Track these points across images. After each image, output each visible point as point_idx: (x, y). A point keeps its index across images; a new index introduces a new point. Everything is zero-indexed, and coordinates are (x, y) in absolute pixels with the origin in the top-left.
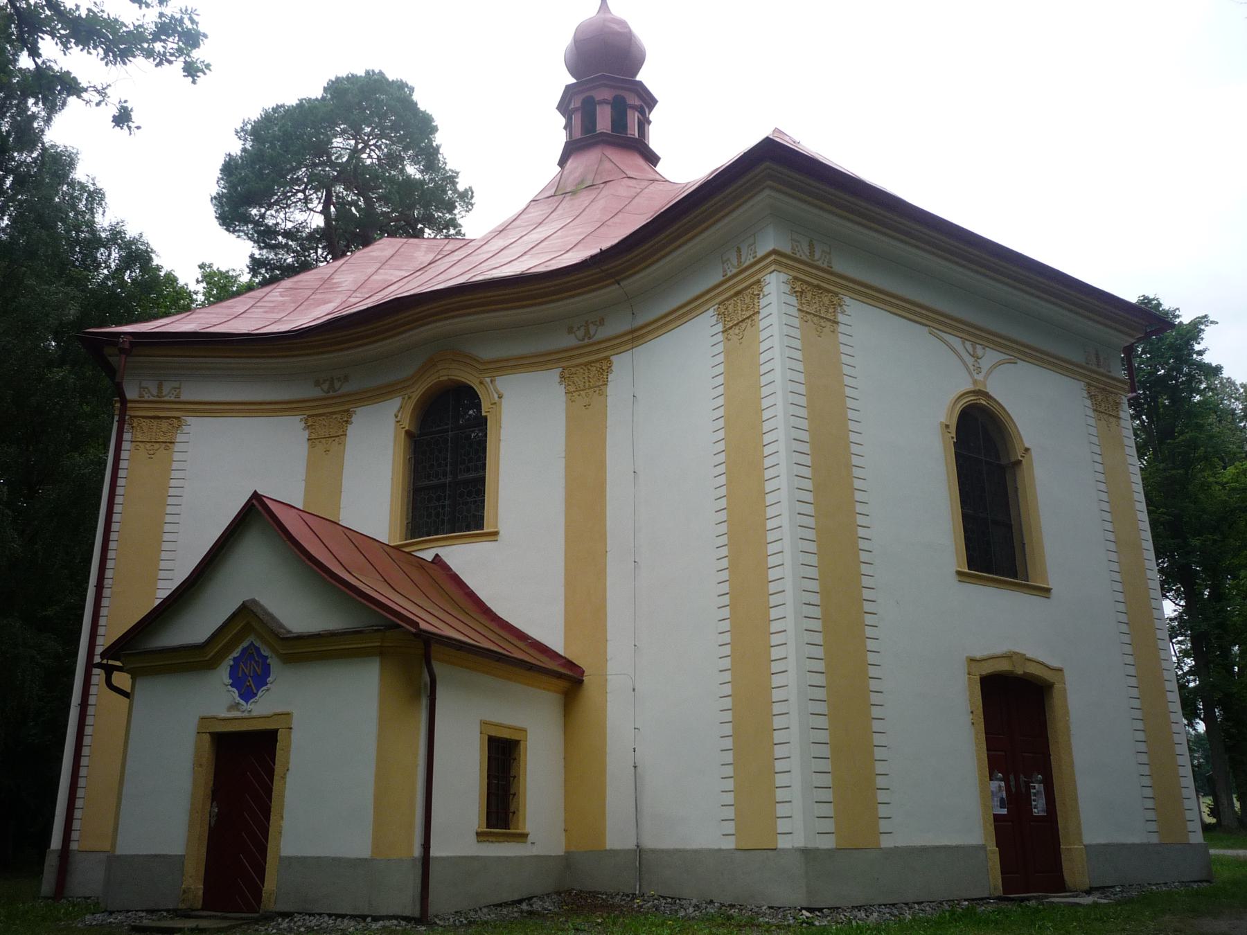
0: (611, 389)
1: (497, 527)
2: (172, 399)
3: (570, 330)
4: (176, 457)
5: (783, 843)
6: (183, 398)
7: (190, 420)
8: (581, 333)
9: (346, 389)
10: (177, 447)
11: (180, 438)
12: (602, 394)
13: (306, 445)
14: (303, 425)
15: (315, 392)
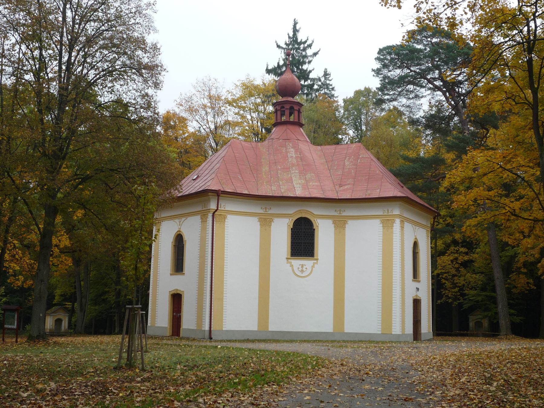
0: (346, 229)
1: (318, 257)
2: (223, 209)
3: (336, 211)
4: (226, 226)
5: (393, 333)
6: (226, 209)
7: (228, 216)
8: (338, 212)
9: (270, 212)
10: (226, 223)
11: (226, 220)
12: (344, 229)
13: (259, 226)
14: (258, 220)
15: (261, 211)
